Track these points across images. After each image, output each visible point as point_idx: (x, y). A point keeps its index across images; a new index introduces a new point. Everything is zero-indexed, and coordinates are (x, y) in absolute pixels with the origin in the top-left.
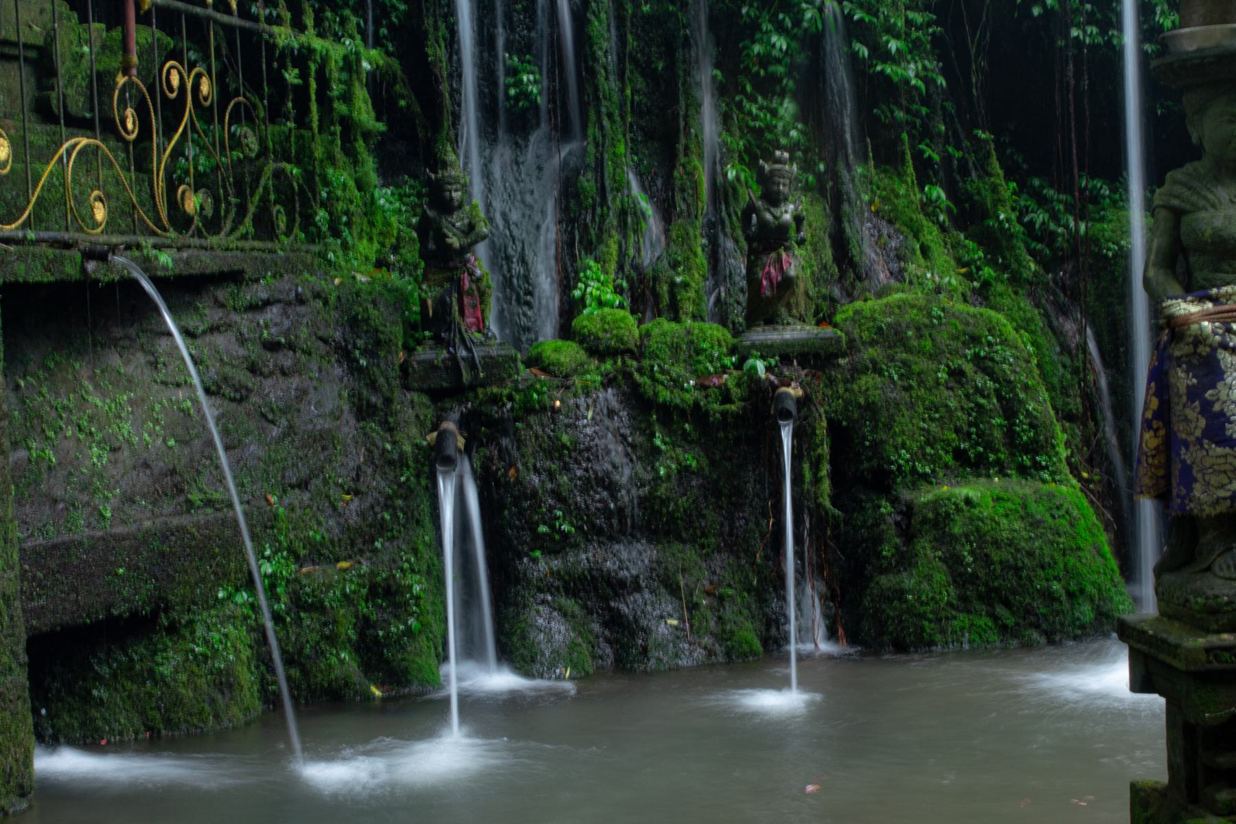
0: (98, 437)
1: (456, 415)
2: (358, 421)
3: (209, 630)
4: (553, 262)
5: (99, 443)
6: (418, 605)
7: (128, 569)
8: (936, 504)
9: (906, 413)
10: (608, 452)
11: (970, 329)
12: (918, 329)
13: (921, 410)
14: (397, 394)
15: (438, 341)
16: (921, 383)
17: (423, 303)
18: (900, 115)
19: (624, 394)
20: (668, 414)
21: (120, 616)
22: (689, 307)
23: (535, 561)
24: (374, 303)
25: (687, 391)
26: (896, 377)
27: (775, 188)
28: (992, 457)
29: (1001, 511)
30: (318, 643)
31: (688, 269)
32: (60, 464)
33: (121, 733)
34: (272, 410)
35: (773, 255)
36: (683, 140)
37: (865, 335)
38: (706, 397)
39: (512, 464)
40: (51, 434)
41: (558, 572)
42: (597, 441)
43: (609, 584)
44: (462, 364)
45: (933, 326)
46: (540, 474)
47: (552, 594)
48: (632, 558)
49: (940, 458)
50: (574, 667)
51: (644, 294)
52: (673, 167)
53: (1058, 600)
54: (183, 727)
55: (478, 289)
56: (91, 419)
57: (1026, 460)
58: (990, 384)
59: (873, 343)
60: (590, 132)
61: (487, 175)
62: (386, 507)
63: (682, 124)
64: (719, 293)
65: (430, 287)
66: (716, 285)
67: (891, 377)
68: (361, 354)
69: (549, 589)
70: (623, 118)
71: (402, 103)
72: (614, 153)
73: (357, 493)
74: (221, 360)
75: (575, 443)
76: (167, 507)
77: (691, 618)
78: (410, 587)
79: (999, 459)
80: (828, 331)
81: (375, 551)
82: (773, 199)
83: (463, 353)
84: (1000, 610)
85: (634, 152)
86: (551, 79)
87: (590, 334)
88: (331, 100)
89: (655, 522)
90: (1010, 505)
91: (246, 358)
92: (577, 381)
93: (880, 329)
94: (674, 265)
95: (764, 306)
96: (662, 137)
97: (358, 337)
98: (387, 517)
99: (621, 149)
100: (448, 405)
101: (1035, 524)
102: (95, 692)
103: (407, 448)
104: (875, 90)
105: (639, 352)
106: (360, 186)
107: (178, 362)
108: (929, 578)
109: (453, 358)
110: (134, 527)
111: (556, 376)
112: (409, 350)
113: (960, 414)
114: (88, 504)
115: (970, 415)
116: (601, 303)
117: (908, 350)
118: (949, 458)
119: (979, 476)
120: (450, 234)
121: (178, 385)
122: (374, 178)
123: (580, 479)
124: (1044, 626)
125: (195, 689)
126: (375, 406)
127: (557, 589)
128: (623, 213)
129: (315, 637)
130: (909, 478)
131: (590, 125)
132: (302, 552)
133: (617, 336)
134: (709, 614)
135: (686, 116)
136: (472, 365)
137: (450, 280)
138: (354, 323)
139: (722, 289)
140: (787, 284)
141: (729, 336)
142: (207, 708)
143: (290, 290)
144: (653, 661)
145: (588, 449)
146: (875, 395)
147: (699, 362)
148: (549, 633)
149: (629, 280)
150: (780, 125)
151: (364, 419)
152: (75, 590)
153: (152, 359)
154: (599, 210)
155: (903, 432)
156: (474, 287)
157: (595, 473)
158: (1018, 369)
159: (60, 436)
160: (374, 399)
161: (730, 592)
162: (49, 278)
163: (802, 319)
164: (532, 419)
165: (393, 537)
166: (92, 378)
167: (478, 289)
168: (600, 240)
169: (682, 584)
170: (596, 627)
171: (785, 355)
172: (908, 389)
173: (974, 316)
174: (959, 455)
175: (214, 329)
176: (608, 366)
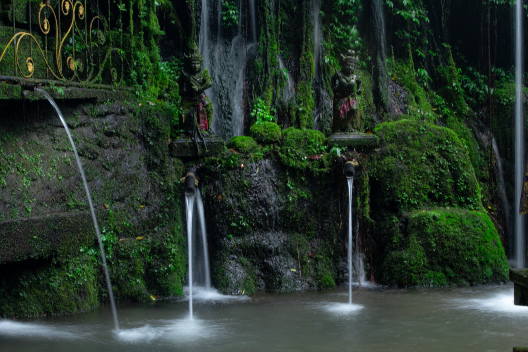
0: (27, 173)
1: (194, 169)
2: (148, 171)
3: (76, 266)
4: (241, 99)
5: (27, 176)
6: (174, 258)
7: (39, 236)
8: (419, 218)
9: (406, 175)
11: (437, 137)
12: (413, 136)
13: (413, 174)
14: (167, 159)
15: (187, 134)
16: (414, 161)
17: (180, 116)
18: (407, 35)
19: (274, 162)
20: (294, 172)
21: (34, 258)
22: (305, 123)
23: (229, 239)
24: (157, 115)
25: (303, 162)
26: (402, 158)
27: (348, 67)
28: (446, 197)
29: (450, 223)
30: (126, 274)
31: (305, 105)
32: (8, 186)
33: (32, 314)
34: (108, 164)
35: (346, 99)
36: (304, 44)
37: (388, 138)
38: (312, 164)
39: (220, 193)
40: (4, 171)
41: (240, 245)
42: (260, 184)
43: (264, 251)
44: (198, 145)
45: (420, 134)
46: (233, 198)
47: (237, 255)
48: (274, 239)
49: (422, 197)
50: (247, 290)
51: (285, 115)
52: (300, 56)
53: (475, 265)
54: (62, 311)
55: (207, 110)
56: (23, 165)
57: (462, 199)
58: (446, 163)
59: (392, 142)
60: (261, 38)
61: (212, 58)
62: (160, 212)
63: (304, 36)
64: (320, 116)
65: (184, 109)
66: (318, 112)
68: (150, 139)
69: (236, 253)
70: (277, 33)
71: (173, 22)
72: (272, 49)
73: (147, 204)
74: (85, 140)
75: (250, 184)
76: (58, 208)
77: (302, 269)
78: (170, 249)
79: (449, 198)
80: (371, 135)
81: (154, 232)
82: (347, 73)
83: (198, 140)
84: (448, 269)
85: (281, 49)
86: (243, 13)
87: (259, 133)
88: (139, 19)
89: (286, 223)
90: (454, 220)
91: (97, 139)
92: (252, 155)
93: (395, 135)
94: (299, 102)
95: (341, 123)
96: (295, 42)
97: (149, 131)
98: (161, 216)
99: (275, 47)
100: (191, 165)
101: (466, 229)
102: (21, 294)
103: (171, 184)
104: (396, 23)
105: (281, 143)
106: (152, 60)
107: (64, 140)
108: (415, 253)
109: (194, 142)
110: (42, 217)
111: (242, 153)
112: (173, 138)
113: (432, 176)
114: (20, 205)
115: (436, 177)
116: (264, 119)
117: (408, 145)
118: (426, 197)
119: (440, 206)
120: (194, 84)
121: (64, 151)
122: (159, 57)
123: (252, 201)
124: (469, 278)
125: (68, 294)
126: (156, 164)
127: (240, 253)
128: (275, 77)
129: (125, 271)
130: (407, 206)
131: (261, 35)
132: (120, 232)
133: (271, 135)
134: (310, 267)
135: (306, 33)
136: (202, 146)
137: (194, 106)
138: (147, 125)
139: (321, 114)
140: (352, 113)
141: (324, 136)
142: (74, 303)
143: (118, 108)
144: (283, 288)
145: (256, 187)
146: (392, 166)
147: (310, 148)
148: (235, 273)
149: (277, 109)
150: (351, 38)
151: (151, 170)
152: (13, 245)
153: (52, 138)
154: (264, 76)
155: (405, 184)
156: (205, 109)
157: (259, 198)
158: (460, 156)
159: (8, 173)
160: (156, 161)
161: (321, 257)
162: (6, 97)
163: (358, 129)
164: (230, 172)
165: (163, 226)
166: (24, 146)
167: (207, 110)
168: (264, 90)
169: (298, 252)
170: (257, 271)
171: (350, 146)
172: (407, 164)
173: (440, 130)
174: (431, 196)
175: (82, 125)
176: (266, 149)
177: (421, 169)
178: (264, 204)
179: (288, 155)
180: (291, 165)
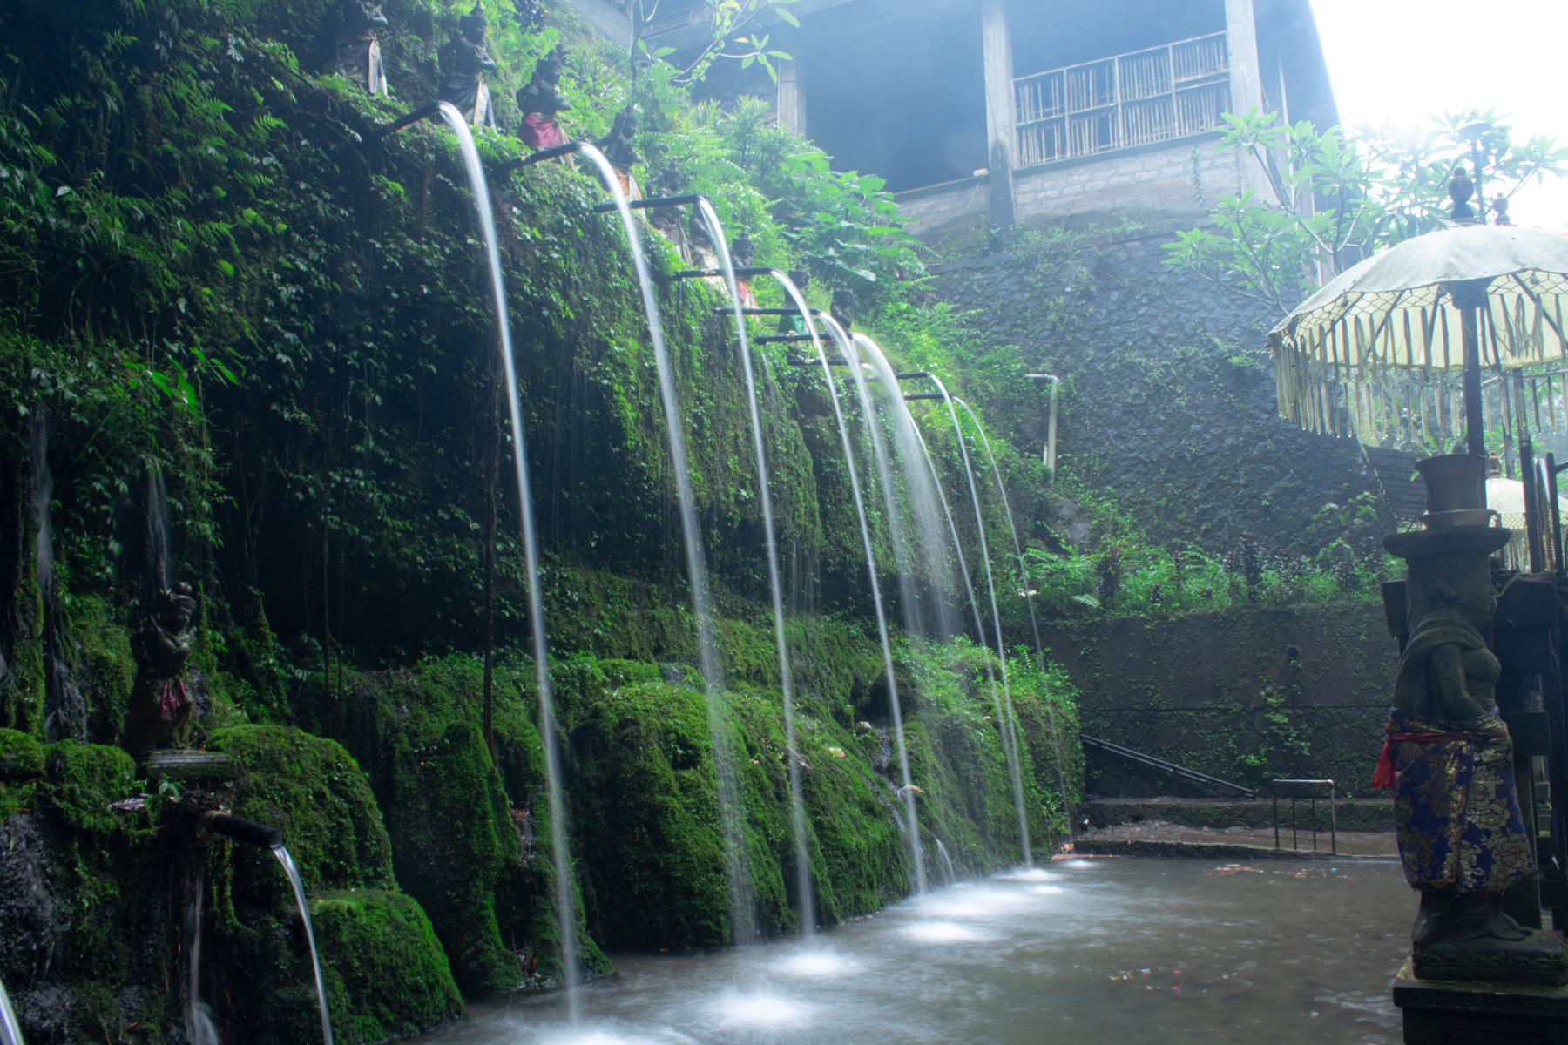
10: (29, 884)
16: (297, 804)
19: (38, 821)
25: (108, 815)
35: (171, 681)
36: (22, 563)
37: (248, 761)
38: (127, 821)
53: (423, 992)
57: (370, 871)
59: (253, 768)
64: (57, 716)
67: (273, 799)
84: (383, 1008)
90: (378, 912)
93: (258, 754)
94: (22, 685)
101: (397, 927)
117: (283, 774)
118: (318, 873)
133: (26, 758)
135: (25, 539)
157: (20, 910)
161: (152, 1026)
169: (104, 1025)
172: (287, 810)
174: (324, 868)
177: (309, 819)
178: (30, 922)
179: (73, 801)
180: (85, 826)
